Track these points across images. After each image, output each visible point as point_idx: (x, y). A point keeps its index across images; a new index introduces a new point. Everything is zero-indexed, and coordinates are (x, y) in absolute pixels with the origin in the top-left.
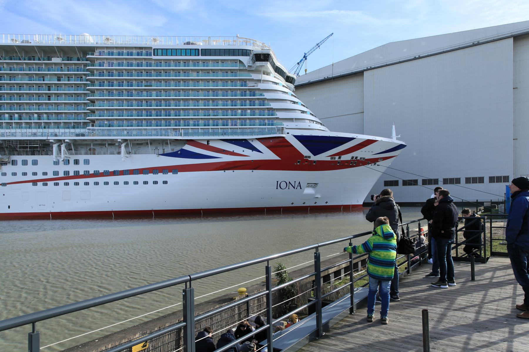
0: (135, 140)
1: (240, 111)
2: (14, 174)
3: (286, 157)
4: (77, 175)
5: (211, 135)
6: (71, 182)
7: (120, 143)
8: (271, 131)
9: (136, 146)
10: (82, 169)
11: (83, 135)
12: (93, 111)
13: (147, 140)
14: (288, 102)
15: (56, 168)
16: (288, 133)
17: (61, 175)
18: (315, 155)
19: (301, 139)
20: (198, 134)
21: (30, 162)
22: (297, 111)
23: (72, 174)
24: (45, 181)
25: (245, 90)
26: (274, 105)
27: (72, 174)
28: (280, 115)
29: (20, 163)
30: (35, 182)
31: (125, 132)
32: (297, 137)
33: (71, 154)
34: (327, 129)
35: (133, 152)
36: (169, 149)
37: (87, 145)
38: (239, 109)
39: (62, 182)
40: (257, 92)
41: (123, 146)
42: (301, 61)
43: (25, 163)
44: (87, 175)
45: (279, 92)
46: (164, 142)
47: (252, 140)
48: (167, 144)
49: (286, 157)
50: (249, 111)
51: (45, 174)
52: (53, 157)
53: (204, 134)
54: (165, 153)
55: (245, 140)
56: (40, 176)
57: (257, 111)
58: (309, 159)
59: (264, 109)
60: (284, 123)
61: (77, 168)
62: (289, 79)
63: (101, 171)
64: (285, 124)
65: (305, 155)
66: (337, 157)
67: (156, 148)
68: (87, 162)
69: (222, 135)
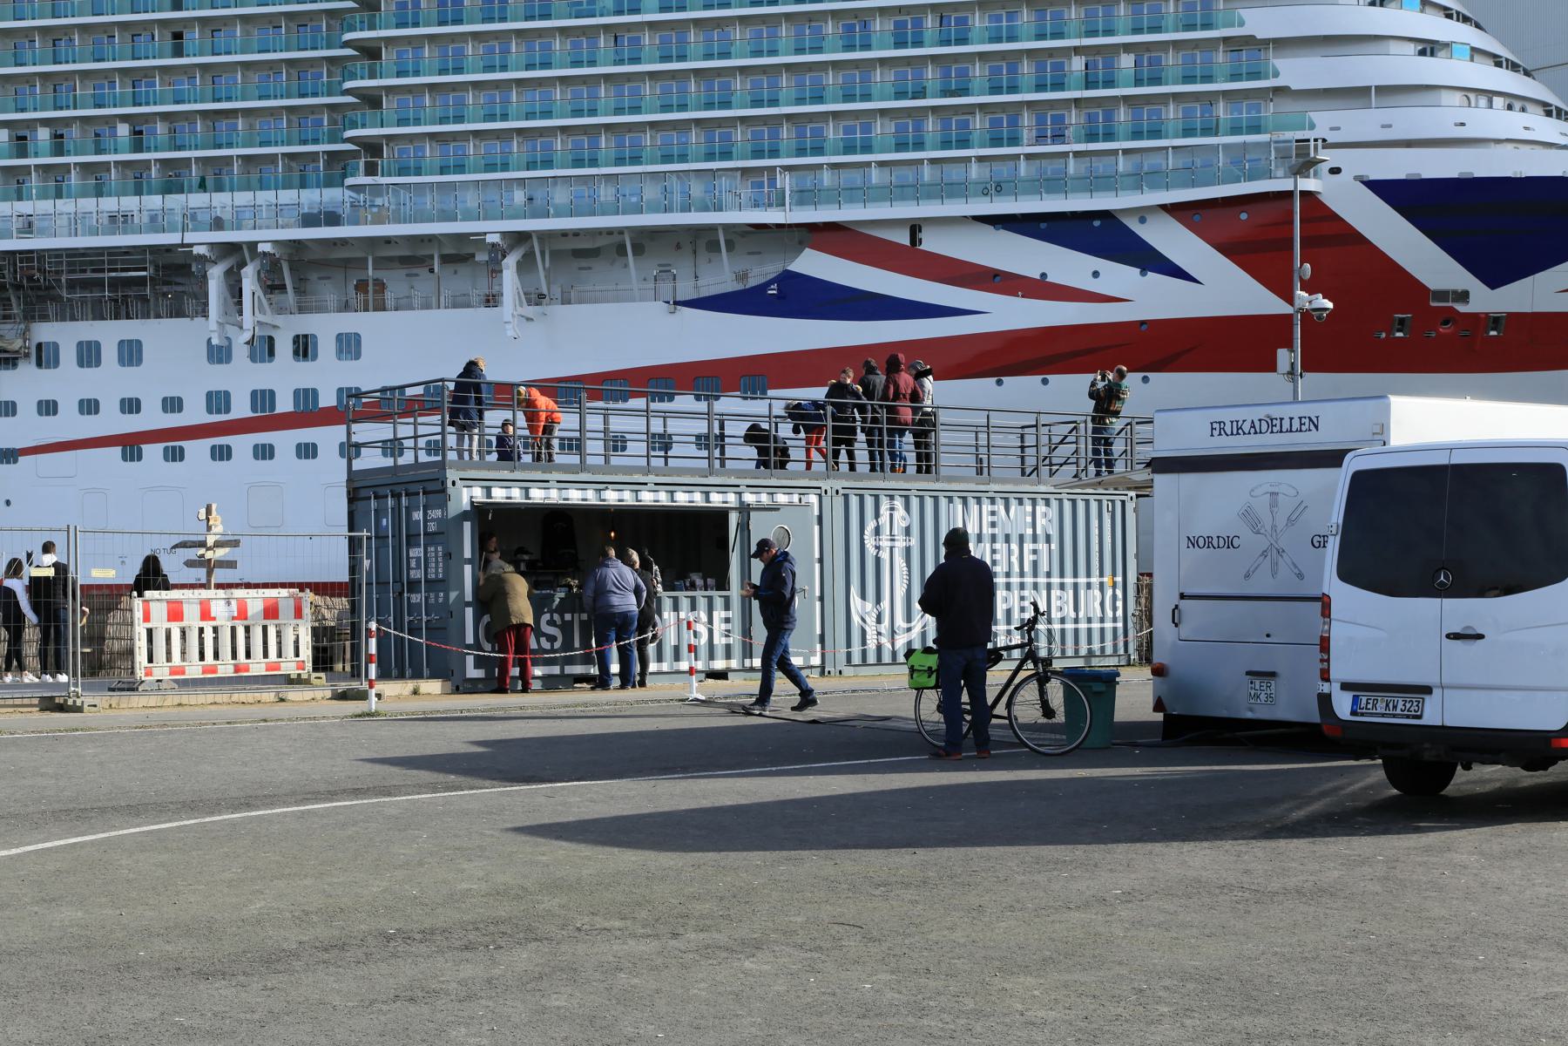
0: (564, 234)
1: (1078, 64)
2: (48, 408)
9: (572, 262)
11: (333, 219)
13: (621, 231)
16: (1335, 171)
17: (241, 409)
19: (1404, 196)
20: (864, 194)
21: (109, 353)
22: (1394, 47)
23: (284, 405)
24: (173, 439)
28: (1294, 71)
29: (68, 355)
30: (131, 445)
31: (519, 196)
32: (1385, 190)
33: (280, 310)
35: (557, 291)
36: (721, 277)
37: (347, 264)
38: (1077, 50)
39: (242, 444)
41: (510, 263)
43: (89, 355)
46: (701, 240)
47: (1142, 213)
48: (714, 247)
51: (173, 404)
52: (210, 326)
53: (892, 193)
54: (705, 293)
56: (152, 418)
57: (1170, 59)
58: (1461, 308)
64: (1325, 122)
65: (1433, 282)
67: (665, 270)
68: (349, 346)
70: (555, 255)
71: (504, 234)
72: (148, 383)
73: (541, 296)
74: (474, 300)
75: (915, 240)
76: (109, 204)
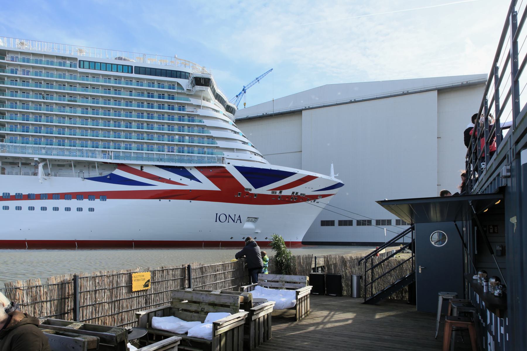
1: (177, 137)
3: (226, 188)
5: (145, 160)
7: (37, 163)
8: (210, 160)
9: (58, 166)
13: (70, 161)
14: (229, 131)
16: (229, 163)
18: (256, 188)
19: (242, 170)
20: (130, 158)
22: (238, 142)
25: (183, 115)
26: (214, 133)
31: (44, 151)
32: (238, 168)
34: (268, 163)
36: (96, 173)
38: (177, 134)
40: (196, 118)
41: (41, 166)
42: (240, 94)
45: (220, 120)
46: (91, 165)
47: (191, 168)
48: (94, 167)
49: (226, 188)
50: (187, 138)
53: (137, 159)
55: (183, 168)
57: (196, 138)
58: (250, 192)
59: (203, 137)
60: (224, 153)
62: (229, 109)
64: (226, 154)
65: (246, 187)
66: (278, 192)
69: (158, 160)
70: (53, 165)
71: (39, 158)
73: (49, 174)
74: (31, 174)
75: (141, 169)
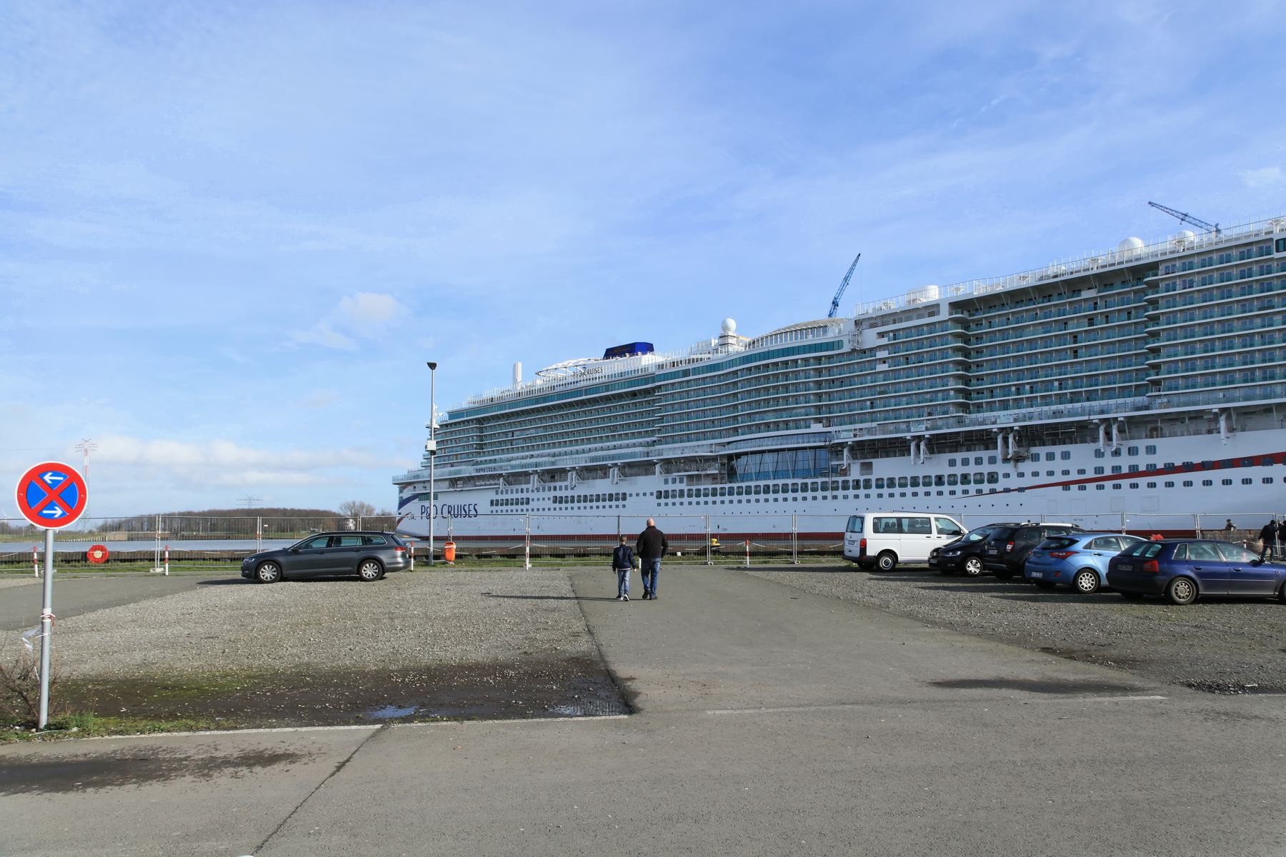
2: (1036, 474)
4: (1134, 473)
6: (1125, 483)
9: (1243, 418)
10: (1142, 461)
12: (1156, 367)
15: (1099, 462)
17: (1108, 472)
21: (1058, 456)
24: (1082, 484)
27: (1125, 470)
29: (1043, 457)
30: (1066, 485)
37: (1147, 423)
39: (1108, 484)
43: (1050, 457)
44: (1152, 471)
51: (1082, 472)
56: (1074, 476)
61: (1133, 460)
63: (1178, 463)
68: (1151, 450)
72: (1072, 466)
76: (1054, 408)
